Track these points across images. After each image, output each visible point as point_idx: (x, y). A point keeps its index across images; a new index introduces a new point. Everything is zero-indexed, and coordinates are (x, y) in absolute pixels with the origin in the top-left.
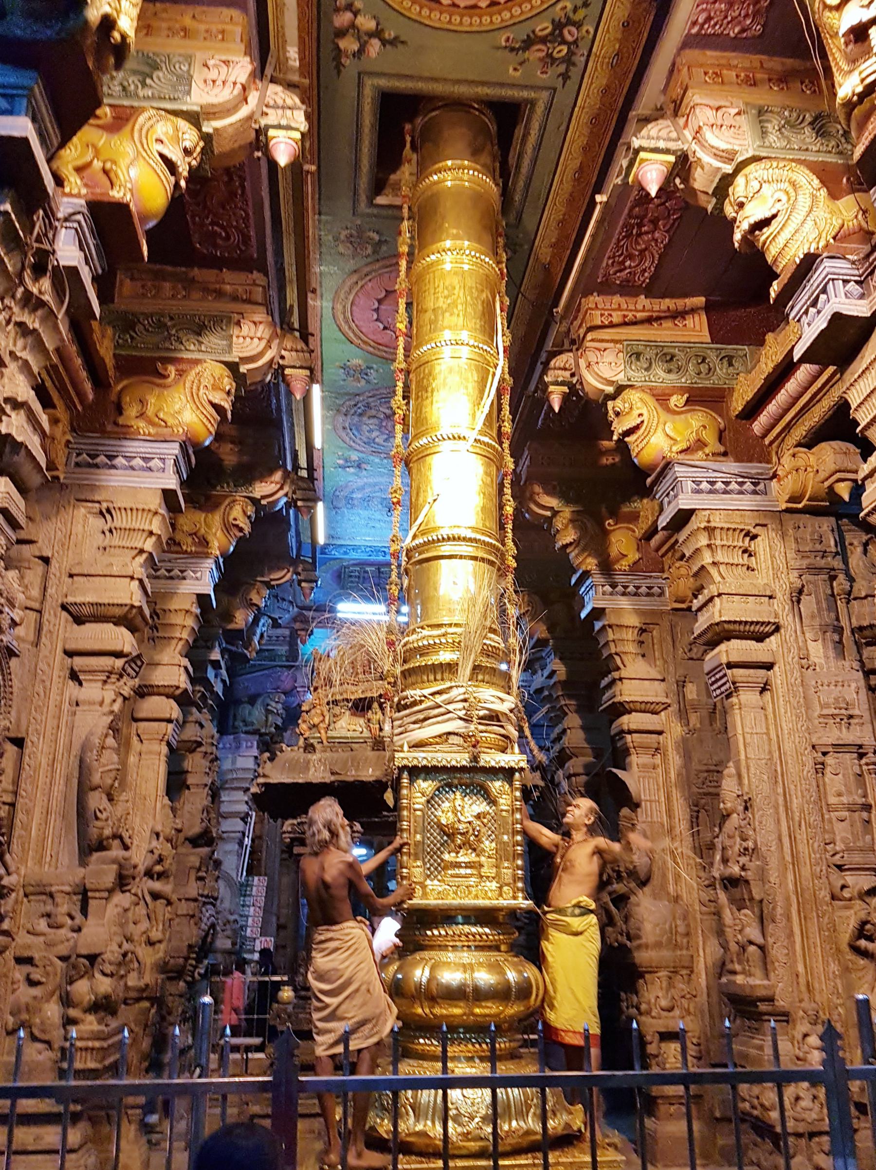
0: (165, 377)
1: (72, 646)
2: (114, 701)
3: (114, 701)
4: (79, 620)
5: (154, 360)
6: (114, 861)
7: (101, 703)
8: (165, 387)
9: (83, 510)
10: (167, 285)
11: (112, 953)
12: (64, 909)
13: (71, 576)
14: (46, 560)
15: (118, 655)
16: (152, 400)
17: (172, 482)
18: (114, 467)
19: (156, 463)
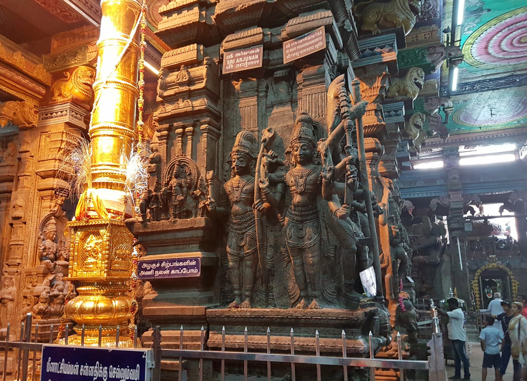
0: (67, 77)
1: (39, 188)
2: (55, 206)
3: (55, 206)
4: (43, 178)
5: (62, 71)
6: (45, 264)
7: (50, 207)
8: (67, 81)
9: (44, 136)
10: (68, 39)
11: (44, 294)
12: (35, 280)
13: (39, 161)
14: (32, 156)
15: (52, 189)
16: (62, 88)
17: (67, 119)
18: (52, 117)
19: (65, 112)
